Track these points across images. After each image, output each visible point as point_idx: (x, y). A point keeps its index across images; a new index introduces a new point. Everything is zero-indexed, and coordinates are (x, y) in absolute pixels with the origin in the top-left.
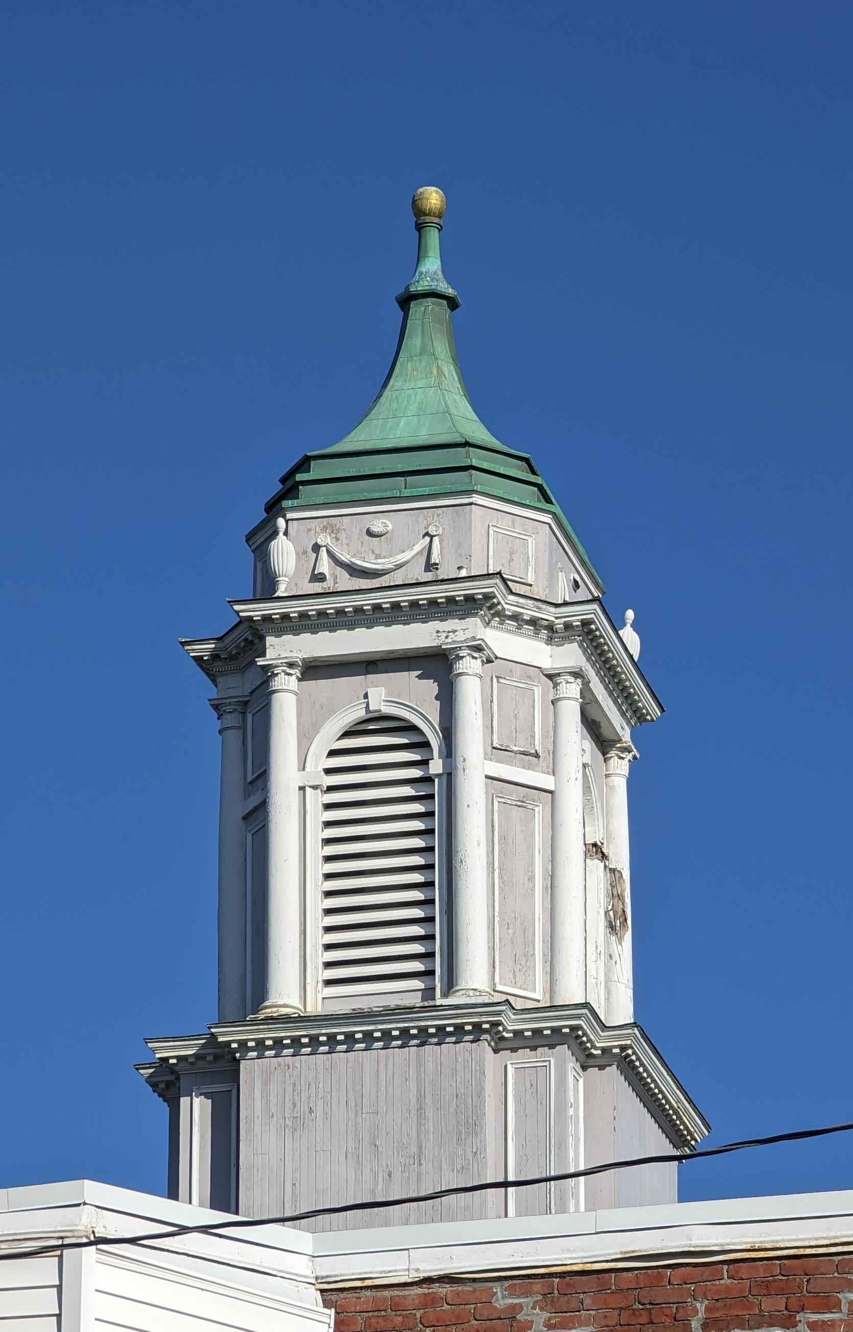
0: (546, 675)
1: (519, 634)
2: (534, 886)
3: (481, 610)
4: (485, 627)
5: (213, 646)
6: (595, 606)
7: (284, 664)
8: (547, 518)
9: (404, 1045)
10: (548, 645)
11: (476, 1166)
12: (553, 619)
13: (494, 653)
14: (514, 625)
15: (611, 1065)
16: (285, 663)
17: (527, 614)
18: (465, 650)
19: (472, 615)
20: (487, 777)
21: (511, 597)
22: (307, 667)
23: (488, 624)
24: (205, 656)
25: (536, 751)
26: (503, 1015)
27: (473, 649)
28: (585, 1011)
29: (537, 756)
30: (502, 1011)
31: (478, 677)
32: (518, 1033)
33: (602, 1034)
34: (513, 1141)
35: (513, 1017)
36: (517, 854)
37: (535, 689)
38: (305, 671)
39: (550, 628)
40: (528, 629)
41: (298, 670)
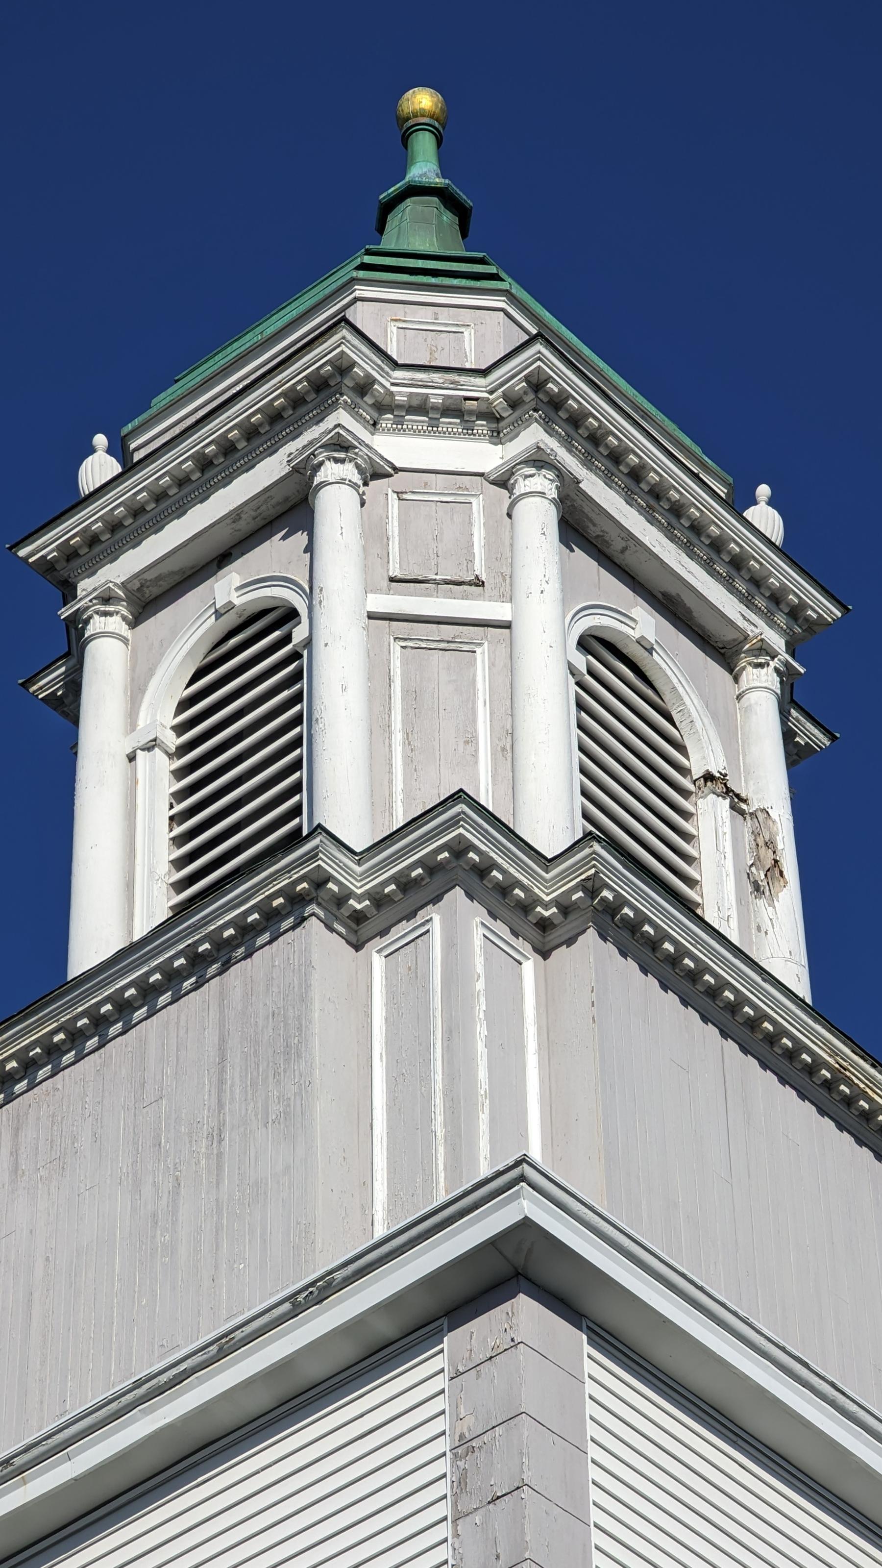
0: (494, 483)
1: (437, 434)
2: (476, 751)
3: (342, 394)
4: (373, 434)
5: (63, 669)
6: (538, 347)
7: (94, 601)
8: (500, 302)
9: (201, 980)
10: (496, 444)
11: (298, 1103)
12: (486, 395)
13: (386, 460)
14: (423, 422)
15: (584, 931)
16: (95, 598)
17: (436, 397)
18: (321, 453)
19: (331, 408)
20: (372, 616)
21: (399, 374)
22: (144, 604)
23: (375, 424)
24: (57, 690)
25: (477, 577)
26: (321, 855)
27: (333, 447)
28: (461, 807)
29: (478, 583)
30: (317, 847)
31: (348, 485)
32: (379, 900)
33: (548, 876)
34: (382, 1061)
35: (359, 869)
36: (441, 711)
37: (473, 500)
38: (140, 611)
39: (491, 416)
40: (450, 423)
41: (122, 606)
